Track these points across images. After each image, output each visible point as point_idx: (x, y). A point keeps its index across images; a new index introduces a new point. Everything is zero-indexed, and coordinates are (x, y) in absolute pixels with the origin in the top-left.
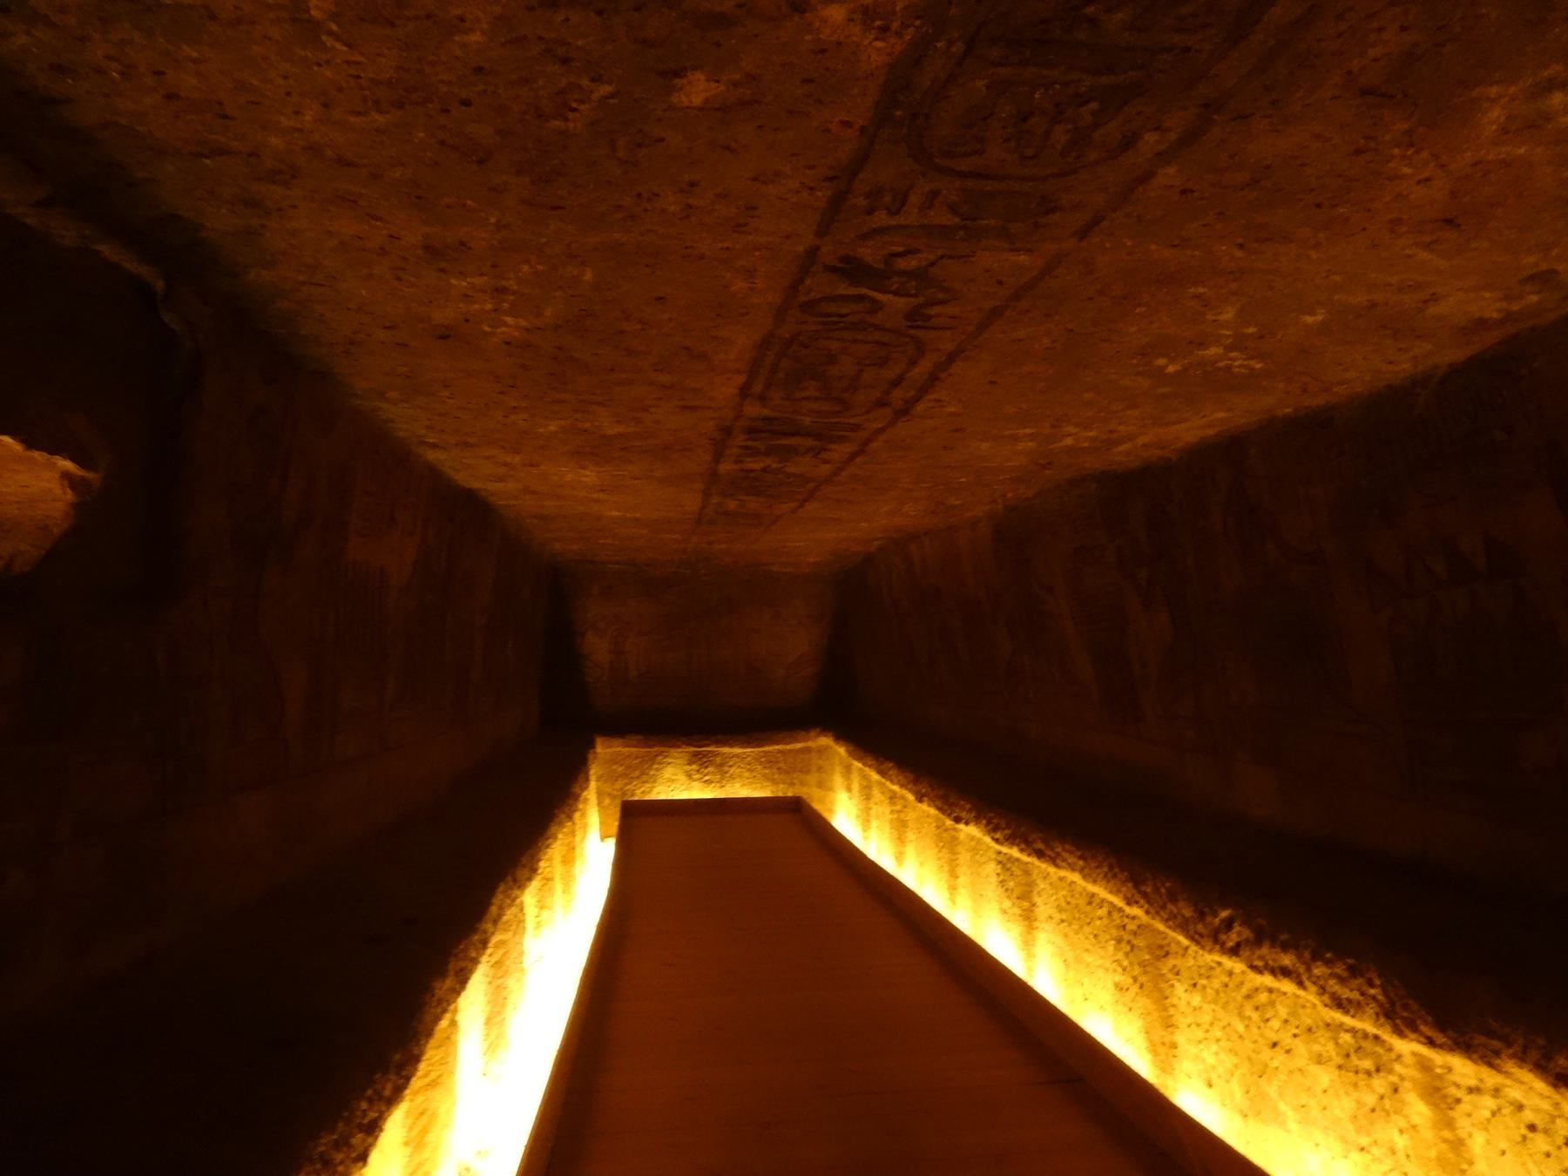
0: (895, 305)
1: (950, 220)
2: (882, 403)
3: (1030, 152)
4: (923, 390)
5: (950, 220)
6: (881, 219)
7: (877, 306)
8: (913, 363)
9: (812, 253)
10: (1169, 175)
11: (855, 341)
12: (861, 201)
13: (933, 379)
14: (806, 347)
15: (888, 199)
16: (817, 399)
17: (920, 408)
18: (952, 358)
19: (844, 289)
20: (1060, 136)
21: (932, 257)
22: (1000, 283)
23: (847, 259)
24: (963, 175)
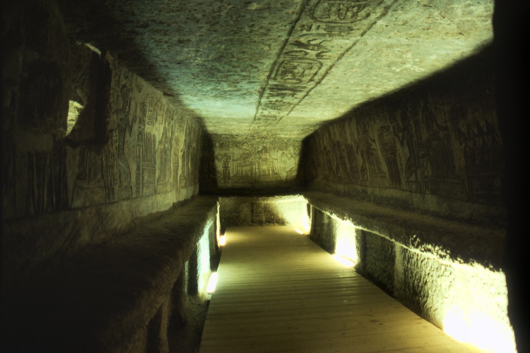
0: (312, 53)
1: (323, 32)
2: (311, 80)
3: (342, 18)
4: (324, 77)
5: (323, 32)
6: (305, 32)
7: (307, 54)
8: (320, 68)
9: (287, 40)
10: (380, 22)
11: (301, 62)
12: (299, 28)
13: (327, 73)
14: (287, 64)
15: (306, 27)
16: (291, 79)
17: (324, 81)
18: (331, 67)
19: (296, 49)
20: (349, 14)
21: (321, 41)
22: (341, 47)
23: (296, 42)
24: (326, 22)
